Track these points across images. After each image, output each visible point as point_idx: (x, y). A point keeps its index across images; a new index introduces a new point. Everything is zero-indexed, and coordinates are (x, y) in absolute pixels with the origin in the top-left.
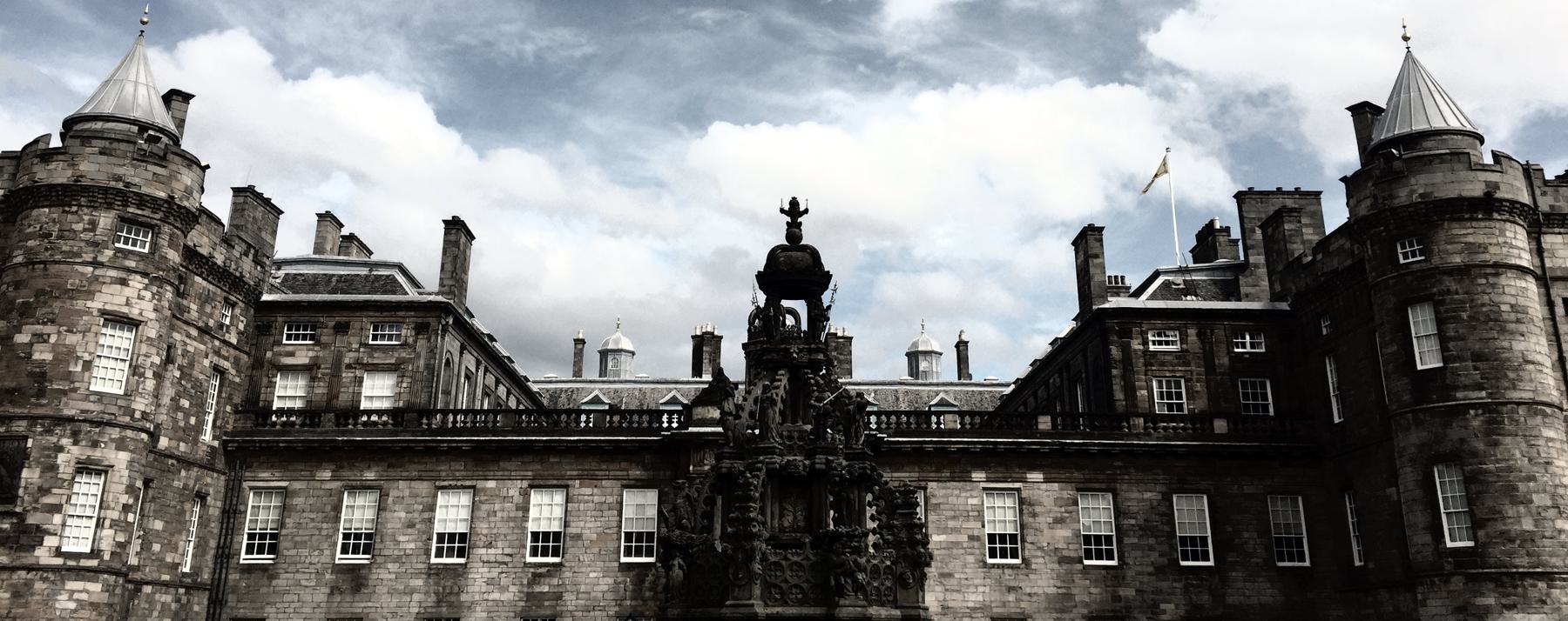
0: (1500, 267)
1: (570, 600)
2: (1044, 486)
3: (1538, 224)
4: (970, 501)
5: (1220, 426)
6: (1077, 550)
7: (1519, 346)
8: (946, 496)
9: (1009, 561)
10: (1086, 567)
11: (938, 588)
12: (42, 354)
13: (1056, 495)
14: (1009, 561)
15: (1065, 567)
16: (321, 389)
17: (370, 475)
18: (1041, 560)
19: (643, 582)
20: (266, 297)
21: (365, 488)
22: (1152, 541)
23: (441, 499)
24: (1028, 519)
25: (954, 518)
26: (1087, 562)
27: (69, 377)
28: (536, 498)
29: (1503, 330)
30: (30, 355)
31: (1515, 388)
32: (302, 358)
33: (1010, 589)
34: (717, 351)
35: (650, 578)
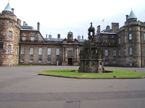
0: (138, 31)
1: (52, 58)
3: (141, 27)
5: (110, 44)
7: (138, 38)
12: (4, 35)
16: (27, 38)
17: (33, 47)
20: (21, 30)
21: (32, 47)
23: (39, 49)
27: (6, 37)
28: (48, 49)
30: (2, 35)
32: (25, 35)
34: (60, 36)
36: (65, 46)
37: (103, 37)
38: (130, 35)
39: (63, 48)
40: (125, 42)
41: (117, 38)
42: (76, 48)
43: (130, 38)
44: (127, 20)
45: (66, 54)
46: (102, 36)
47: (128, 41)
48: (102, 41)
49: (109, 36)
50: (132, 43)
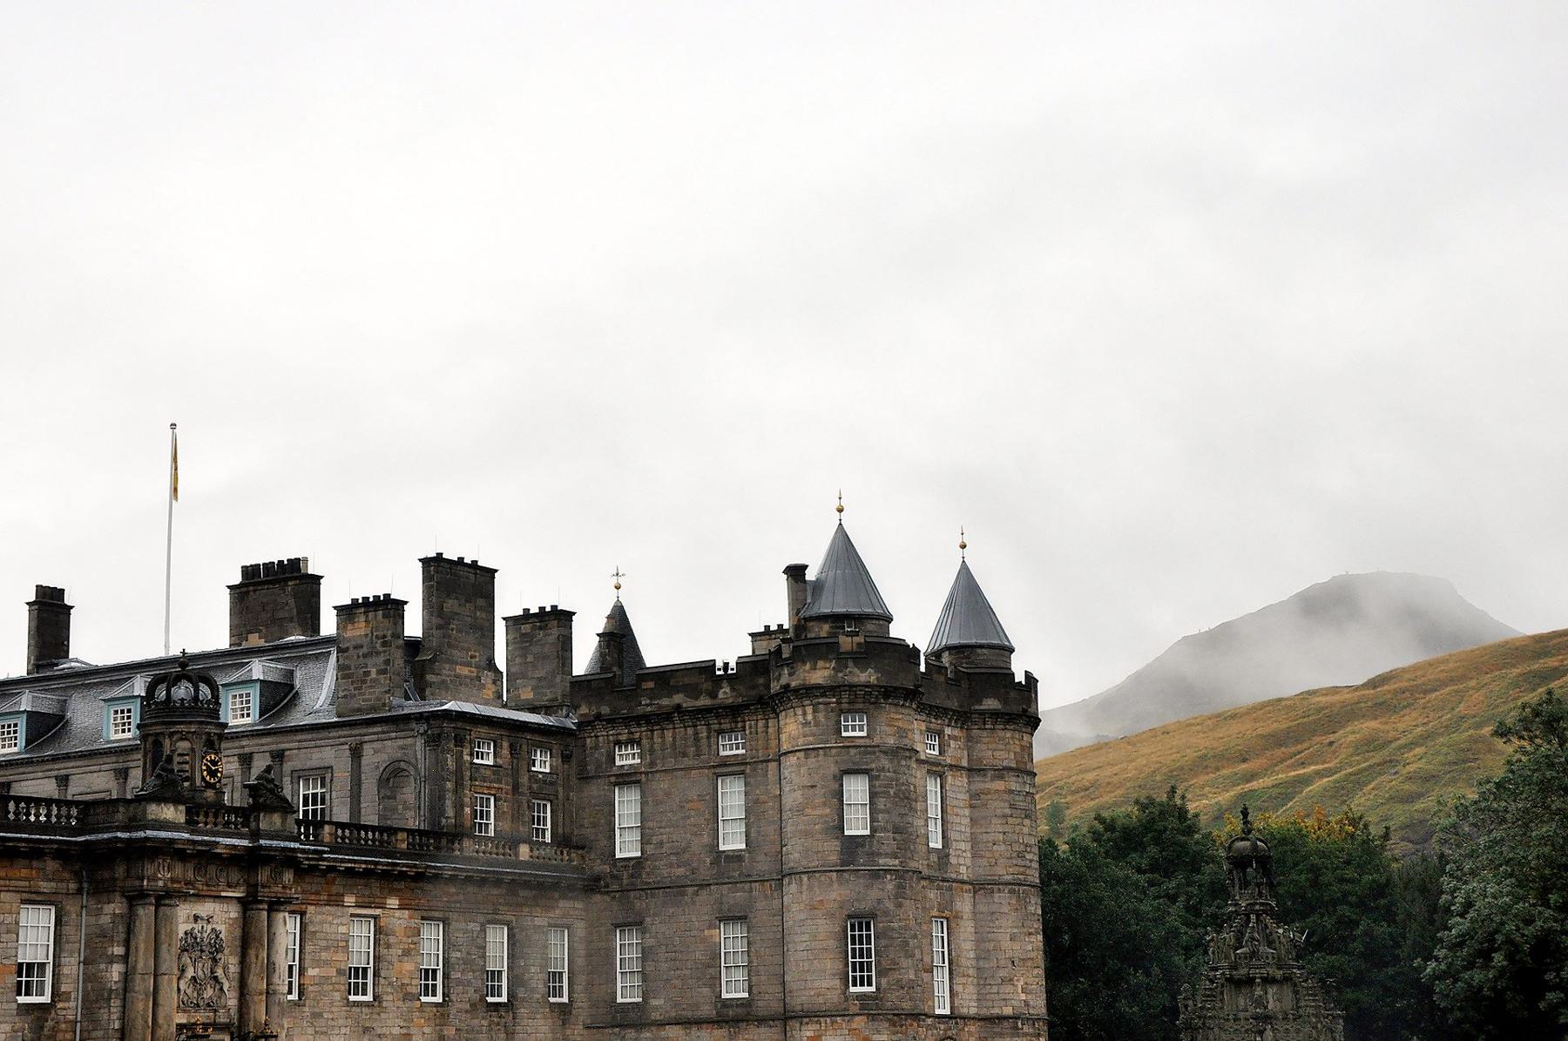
2: (398, 914)
4: (342, 929)
5: (524, 851)
6: (416, 984)
8: (322, 923)
9: (360, 998)
10: (422, 1004)
11: (310, 1031)
13: (404, 923)
14: (360, 998)
15: (408, 1004)
18: (390, 998)
19: (42, 1028)
22: (470, 975)
24: (384, 951)
25: (327, 948)
26: (423, 999)
29: (911, 809)
31: (912, 858)
33: (366, 1030)
35: (50, 1023)
36: (162, 875)
37: (467, 758)
38: (856, 790)
39: (135, 897)
40: (732, 840)
41: (584, 778)
42: (275, 906)
43: (857, 825)
44: (802, 623)
45: (169, 998)
46: (460, 742)
47: (831, 850)
48: (459, 807)
49: (511, 746)
50: (876, 875)
